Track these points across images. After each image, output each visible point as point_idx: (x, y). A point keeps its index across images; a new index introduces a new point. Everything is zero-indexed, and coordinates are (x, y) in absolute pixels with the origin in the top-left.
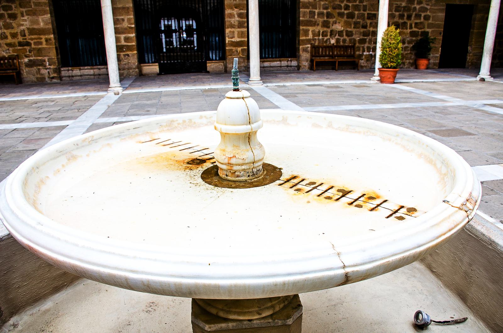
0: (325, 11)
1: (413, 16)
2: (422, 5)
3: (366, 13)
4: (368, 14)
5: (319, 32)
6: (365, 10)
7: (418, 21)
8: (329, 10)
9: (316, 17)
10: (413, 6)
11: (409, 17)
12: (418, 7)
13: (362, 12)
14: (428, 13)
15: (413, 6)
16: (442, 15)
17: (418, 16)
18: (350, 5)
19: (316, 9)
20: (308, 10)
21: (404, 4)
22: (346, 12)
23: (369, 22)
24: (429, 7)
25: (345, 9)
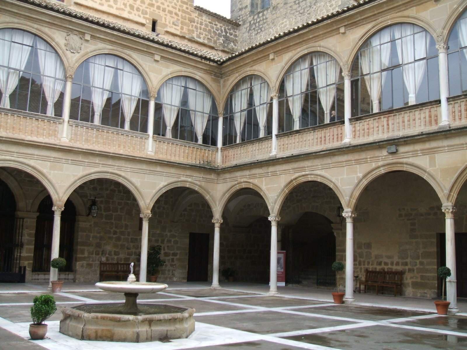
0: (98, 235)
1: (166, 240)
2: (172, 233)
3: (130, 237)
4: (131, 238)
5: (93, 251)
6: (128, 235)
7: (170, 245)
8: (101, 235)
9: (91, 239)
10: (165, 233)
11: (163, 242)
12: (169, 234)
13: (126, 236)
14: (177, 239)
15: (165, 233)
16: (187, 241)
17: (169, 241)
18: (118, 231)
19: (91, 233)
20: (85, 234)
21: (158, 232)
22: (114, 236)
23: (132, 245)
24: (177, 235)
25: (114, 234)
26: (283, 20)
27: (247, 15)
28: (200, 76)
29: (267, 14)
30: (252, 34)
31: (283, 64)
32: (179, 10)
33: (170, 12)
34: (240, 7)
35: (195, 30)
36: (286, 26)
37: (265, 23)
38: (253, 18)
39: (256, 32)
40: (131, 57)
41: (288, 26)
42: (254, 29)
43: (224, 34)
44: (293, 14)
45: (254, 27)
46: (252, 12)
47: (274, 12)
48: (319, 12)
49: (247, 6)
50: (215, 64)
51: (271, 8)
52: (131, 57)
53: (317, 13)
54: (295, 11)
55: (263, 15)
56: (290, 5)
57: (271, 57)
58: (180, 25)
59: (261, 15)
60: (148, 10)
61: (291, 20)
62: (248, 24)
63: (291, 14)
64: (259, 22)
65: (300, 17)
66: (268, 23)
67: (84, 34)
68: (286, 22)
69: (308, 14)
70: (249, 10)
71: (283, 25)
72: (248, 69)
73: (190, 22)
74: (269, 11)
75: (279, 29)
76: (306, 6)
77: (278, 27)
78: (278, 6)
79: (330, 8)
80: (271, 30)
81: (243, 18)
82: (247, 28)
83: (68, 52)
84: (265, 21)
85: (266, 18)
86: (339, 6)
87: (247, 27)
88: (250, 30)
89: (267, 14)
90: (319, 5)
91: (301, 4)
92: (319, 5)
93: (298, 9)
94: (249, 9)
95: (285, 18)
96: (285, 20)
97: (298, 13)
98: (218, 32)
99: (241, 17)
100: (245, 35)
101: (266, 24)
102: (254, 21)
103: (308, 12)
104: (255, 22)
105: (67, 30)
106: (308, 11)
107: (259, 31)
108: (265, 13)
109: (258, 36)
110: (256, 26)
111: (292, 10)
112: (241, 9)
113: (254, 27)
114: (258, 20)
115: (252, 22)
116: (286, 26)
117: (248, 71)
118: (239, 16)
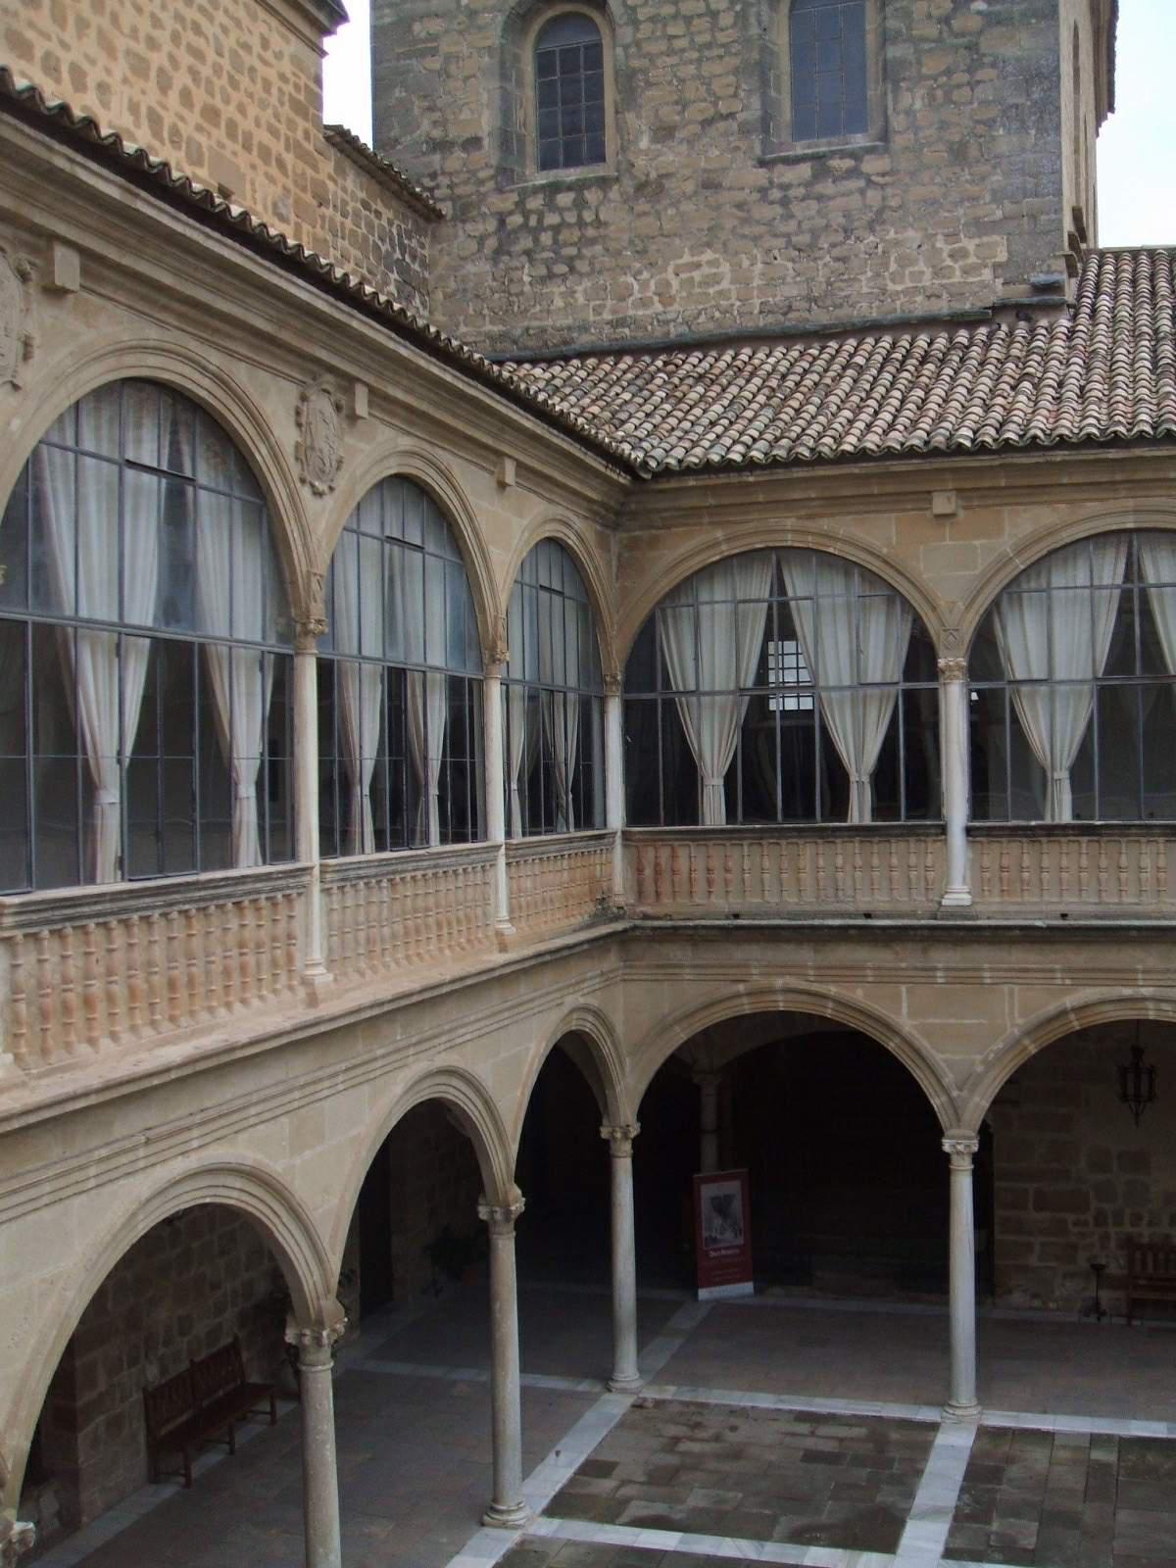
26: (695, 250)
27: (482, 182)
28: (578, 535)
29: (601, 203)
30: (515, 275)
31: (1006, 544)
32: (287, 149)
33: (265, 153)
34: (437, 133)
35: (329, 237)
36: (715, 279)
37: (593, 241)
38: (520, 205)
39: (543, 271)
40: (449, 481)
41: (725, 284)
42: (528, 253)
43: (398, 255)
44: (756, 239)
45: (526, 242)
46: (505, 174)
47: (642, 206)
48: (893, 267)
49: (474, 143)
50: (623, 479)
51: (628, 185)
52: (449, 481)
53: (886, 266)
54: (763, 229)
55: (580, 204)
56: (740, 196)
57: (942, 504)
58: (293, 218)
59: (565, 199)
60: (202, 139)
61: (746, 263)
62: (492, 225)
63: (744, 236)
64: (556, 229)
65: (793, 260)
66: (613, 245)
67: (348, 382)
68: (712, 263)
69: (837, 259)
70: (494, 162)
71: (697, 275)
72: (790, 523)
73: (315, 203)
74: (614, 193)
75: (675, 283)
76: (824, 222)
77: (670, 275)
78: (667, 184)
79: (949, 262)
80: (630, 280)
81: (459, 191)
82: (481, 240)
83: (305, 492)
84: (591, 232)
85: (599, 223)
86: (996, 266)
87: (481, 240)
88: (499, 252)
89: (601, 203)
90: (892, 234)
91: (796, 208)
92: (892, 234)
93: (783, 228)
94: (489, 153)
95: (709, 245)
96: (708, 255)
97: (781, 242)
98: (383, 249)
99: (444, 181)
100: (471, 268)
101: (598, 248)
102: (526, 217)
103: (836, 252)
104: (533, 221)
105: (303, 370)
106: (833, 245)
107: (564, 269)
108: (592, 196)
109: (556, 289)
110: (536, 241)
111: (745, 221)
112: (442, 146)
113: (526, 242)
114: (552, 219)
115: (516, 220)
116: (715, 279)
117: (788, 528)
118: (433, 176)
